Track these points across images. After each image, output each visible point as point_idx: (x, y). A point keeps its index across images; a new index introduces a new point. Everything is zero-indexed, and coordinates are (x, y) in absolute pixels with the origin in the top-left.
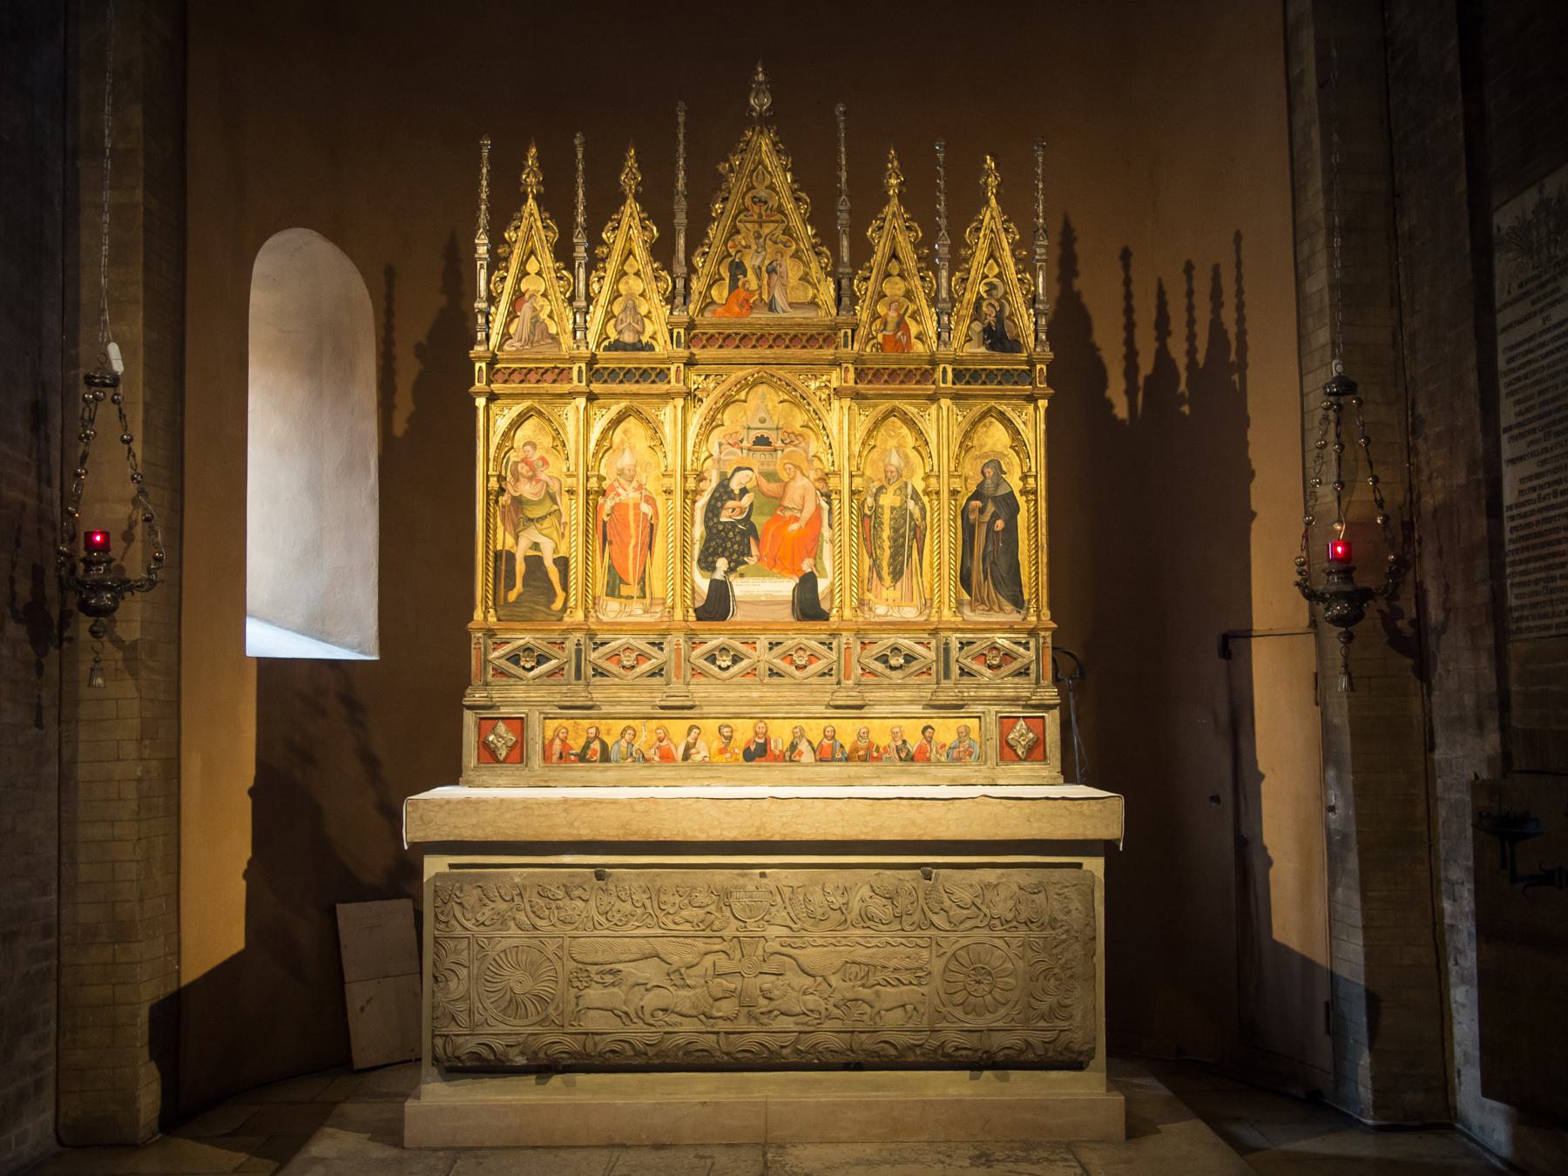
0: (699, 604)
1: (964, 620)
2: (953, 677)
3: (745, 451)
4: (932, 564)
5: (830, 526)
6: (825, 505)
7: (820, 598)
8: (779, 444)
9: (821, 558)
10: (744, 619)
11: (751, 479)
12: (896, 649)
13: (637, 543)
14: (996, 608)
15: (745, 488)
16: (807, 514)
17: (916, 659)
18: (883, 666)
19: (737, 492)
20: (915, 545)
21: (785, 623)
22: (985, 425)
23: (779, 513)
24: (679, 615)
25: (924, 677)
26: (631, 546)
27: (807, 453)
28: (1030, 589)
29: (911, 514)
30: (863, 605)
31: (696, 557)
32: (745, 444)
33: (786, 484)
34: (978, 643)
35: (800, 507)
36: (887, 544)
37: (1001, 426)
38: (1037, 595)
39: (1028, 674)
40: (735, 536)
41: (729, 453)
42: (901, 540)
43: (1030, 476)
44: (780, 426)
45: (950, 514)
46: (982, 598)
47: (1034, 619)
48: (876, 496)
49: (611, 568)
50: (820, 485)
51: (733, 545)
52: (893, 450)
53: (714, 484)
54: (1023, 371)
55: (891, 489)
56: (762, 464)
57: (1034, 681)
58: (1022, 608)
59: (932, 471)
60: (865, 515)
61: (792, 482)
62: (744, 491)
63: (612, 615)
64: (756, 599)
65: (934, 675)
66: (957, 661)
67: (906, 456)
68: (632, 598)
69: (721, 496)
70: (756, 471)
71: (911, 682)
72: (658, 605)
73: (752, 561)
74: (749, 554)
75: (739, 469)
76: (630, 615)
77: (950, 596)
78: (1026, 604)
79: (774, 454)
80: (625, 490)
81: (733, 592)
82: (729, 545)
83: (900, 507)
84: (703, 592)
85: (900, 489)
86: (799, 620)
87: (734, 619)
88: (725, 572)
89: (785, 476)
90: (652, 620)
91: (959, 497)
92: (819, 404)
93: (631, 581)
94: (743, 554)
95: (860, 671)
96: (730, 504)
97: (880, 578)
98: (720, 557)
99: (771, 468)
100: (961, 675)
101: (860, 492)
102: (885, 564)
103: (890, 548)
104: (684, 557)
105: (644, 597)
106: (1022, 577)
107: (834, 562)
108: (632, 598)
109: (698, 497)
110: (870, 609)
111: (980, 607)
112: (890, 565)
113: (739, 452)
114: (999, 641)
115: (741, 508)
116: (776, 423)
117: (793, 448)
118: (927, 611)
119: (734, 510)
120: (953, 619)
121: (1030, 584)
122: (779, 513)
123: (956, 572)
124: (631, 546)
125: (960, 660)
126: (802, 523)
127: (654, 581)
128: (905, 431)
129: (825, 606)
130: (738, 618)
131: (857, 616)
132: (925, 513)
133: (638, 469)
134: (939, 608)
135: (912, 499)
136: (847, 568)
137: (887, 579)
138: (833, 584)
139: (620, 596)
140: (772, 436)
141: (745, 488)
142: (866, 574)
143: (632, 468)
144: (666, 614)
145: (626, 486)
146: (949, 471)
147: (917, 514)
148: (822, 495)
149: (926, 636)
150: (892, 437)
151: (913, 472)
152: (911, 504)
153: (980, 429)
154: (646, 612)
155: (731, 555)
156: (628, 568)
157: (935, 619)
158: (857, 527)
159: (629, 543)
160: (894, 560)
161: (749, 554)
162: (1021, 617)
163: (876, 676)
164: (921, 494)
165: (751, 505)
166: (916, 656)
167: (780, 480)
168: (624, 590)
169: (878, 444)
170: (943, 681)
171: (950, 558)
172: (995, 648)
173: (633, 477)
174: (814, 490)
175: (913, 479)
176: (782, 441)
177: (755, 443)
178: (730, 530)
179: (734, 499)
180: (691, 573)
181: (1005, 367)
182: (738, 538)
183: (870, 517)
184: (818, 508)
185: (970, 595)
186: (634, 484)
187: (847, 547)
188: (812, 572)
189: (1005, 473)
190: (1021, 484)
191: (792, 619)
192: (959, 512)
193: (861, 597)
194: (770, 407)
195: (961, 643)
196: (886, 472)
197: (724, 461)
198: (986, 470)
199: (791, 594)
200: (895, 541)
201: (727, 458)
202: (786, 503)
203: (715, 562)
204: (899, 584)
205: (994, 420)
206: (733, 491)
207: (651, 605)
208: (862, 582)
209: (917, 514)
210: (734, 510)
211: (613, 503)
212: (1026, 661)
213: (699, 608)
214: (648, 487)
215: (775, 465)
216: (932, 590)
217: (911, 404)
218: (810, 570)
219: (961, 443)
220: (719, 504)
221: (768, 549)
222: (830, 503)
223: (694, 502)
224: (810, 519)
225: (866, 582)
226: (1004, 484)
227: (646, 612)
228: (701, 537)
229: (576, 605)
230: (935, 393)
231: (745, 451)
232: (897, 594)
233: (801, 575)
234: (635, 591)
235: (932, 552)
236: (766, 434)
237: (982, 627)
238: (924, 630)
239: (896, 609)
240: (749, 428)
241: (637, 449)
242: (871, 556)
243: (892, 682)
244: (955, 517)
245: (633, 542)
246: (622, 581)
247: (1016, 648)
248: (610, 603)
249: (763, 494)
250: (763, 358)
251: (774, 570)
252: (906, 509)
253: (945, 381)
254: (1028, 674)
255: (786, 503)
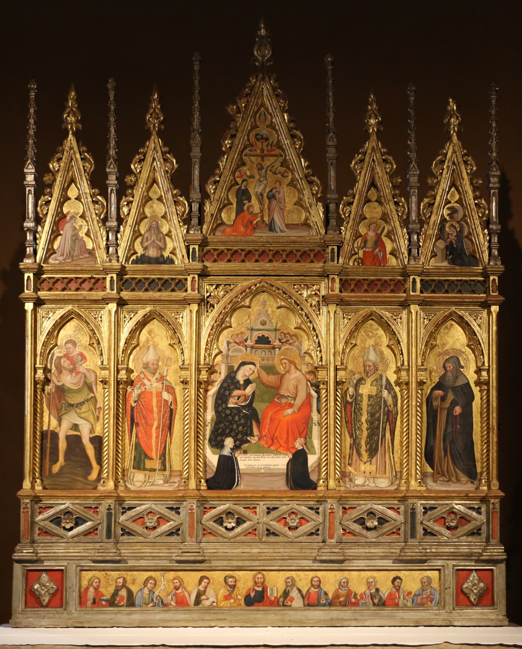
0: (210, 475)
1: (427, 489)
2: (418, 537)
3: (249, 349)
4: (401, 442)
5: (319, 411)
6: (314, 394)
7: (310, 470)
8: (277, 343)
9: (310, 438)
10: (247, 488)
11: (254, 372)
12: (371, 513)
13: (159, 425)
14: (454, 479)
15: (248, 379)
16: (299, 402)
17: (387, 521)
18: (361, 527)
19: (242, 382)
20: (388, 427)
21: (280, 491)
22: (447, 328)
23: (276, 400)
24: (192, 484)
25: (395, 536)
26: (154, 427)
27: (300, 350)
28: (482, 463)
29: (385, 402)
30: (345, 476)
31: (208, 437)
32: (249, 343)
33: (283, 376)
34: (439, 508)
35: (294, 395)
36: (365, 426)
37: (459, 329)
38: (488, 469)
39: (480, 534)
40: (240, 419)
41: (235, 350)
42: (377, 423)
43: (484, 370)
44: (278, 328)
45: (417, 401)
46: (443, 471)
47: (485, 488)
48: (356, 387)
49: (138, 445)
50: (310, 377)
51: (238, 426)
52: (371, 348)
53: (223, 376)
54: (479, 281)
55: (369, 381)
56: (263, 360)
57: (484, 540)
58: (475, 479)
59: (403, 365)
60: (347, 402)
61: (287, 375)
62: (248, 382)
63: (138, 484)
64: (257, 471)
65: (402, 535)
66: (421, 523)
67: (382, 353)
68: (155, 470)
69: (229, 386)
70: (258, 365)
71: (383, 541)
72: (176, 476)
73: (254, 440)
74: (251, 434)
75: (243, 364)
76: (152, 485)
77: (416, 469)
78: (479, 476)
79: (272, 351)
80: (149, 380)
81: (238, 465)
82: (235, 426)
83: (375, 396)
84: (213, 465)
85: (376, 380)
86: (292, 489)
87: (238, 488)
88: (231, 449)
89: (281, 369)
90: (171, 489)
91: (425, 387)
92: (310, 309)
93: (154, 456)
94: (247, 435)
95: (342, 532)
96: (236, 393)
97: (359, 454)
98: (227, 437)
99: (271, 362)
100: (425, 534)
101: (343, 382)
102: (363, 443)
103: (367, 429)
104: (198, 437)
105: (165, 470)
106: (476, 454)
107: (321, 441)
108: (155, 470)
109: (210, 387)
110: (351, 480)
111: (440, 479)
112: (367, 444)
113: (244, 349)
114: (457, 507)
115: (245, 396)
116: (274, 325)
117: (288, 346)
118: (397, 482)
119: (239, 397)
120: (419, 488)
121: (482, 459)
122: (276, 400)
123: (421, 450)
124: (154, 427)
125: (424, 522)
126: (295, 409)
127: (173, 456)
128: (381, 332)
129: (313, 477)
130: (242, 487)
131: (340, 486)
132: (397, 400)
133: (160, 363)
134: (407, 479)
135: (386, 389)
136: (332, 446)
137: (365, 455)
138: (320, 459)
139: (145, 469)
140: (271, 336)
141: (248, 379)
142: (348, 451)
143: (155, 362)
144: (182, 484)
145: (150, 377)
146: (417, 366)
147: (390, 401)
148: (312, 385)
149: (396, 502)
150: (370, 337)
151: (387, 366)
152: (385, 393)
153: (442, 331)
154: (166, 482)
155: (237, 435)
156: (152, 446)
157: (403, 488)
158: (341, 412)
159: (153, 425)
160: (371, 440)
161: (251, 434)
162: (475, 486)
163: (354, 535)
164: (394, 385)
165: (254, 393)
166: (388, 519)
167: (277, 373)
168: (149, 464)
169: (358, 342)
170: (410, 540)
171: (417, 438)
172: (453, 513)
173: (156, 370)
174: (305, 381)
175: (387, 372)
176: (280, 340)
177: (257, 342)
178: (235, 415)
179: (239, 389)
180: (203, 450)
181: (464, 278)
182: (242, 421)
183: (351, 404)
184: (309, 396)
185: (433, 468)
186: (157, 375)
187: (332, 429)
188: (303, 449)
189: (463, 367)
190: (476, 376)
191: (285, 488)
192: (424, 400)
193: (343, 470)
194: (270, 312)
195: (424, 508)
196: (365, 366)
197: (231, 357)
198: (448, 365)
199: (285, 467)
200: (372, 423)
201: (234, 354)
202: (283, 392)
203: (224, 441)
204: (374, 460)
205: (453, 323)
206: (238, 382)
207: (171, 476)
208: (345, 457)
209: (390, 401)
210: (239, 397)
211: (139, 391)
212: (478, 523)
213: (210, 478)
214: (168, 378)
215: (273, 360)
216: (401, 464)
217: (386, 310)
218: (301, 448)
219: (427, 342)
220: (227, 393)
221: (267, 430)
222: (318, 392)
223: (206, 391)
224: (302, 405)
225: (347, 457)
226: (462, 376)
227: (166, 482)
228: (212, 420)
229: (108, 476)
230: (406, 300)
231: (249, 349)
232: (374, 468)
233: (294, 451)
234: (157, 464)
235: (402, 433)
236: (266, 334)
237: (443, 495)
238: (395, 497)
239: (371, 480)
240: (252, 330)
241: (160, 346)
242: (351, 436)
243: (368, 540)
244: (421, 404)
245: (156, 424)
246: (147, 457)
247: (470, 512)
248: (136, 475)
249: (263, 384)
250: (264, 270)
251: (272, 448)
252: (381, 397)
253: (414, 290)
254: (480, 534)
255: (283, 392)
